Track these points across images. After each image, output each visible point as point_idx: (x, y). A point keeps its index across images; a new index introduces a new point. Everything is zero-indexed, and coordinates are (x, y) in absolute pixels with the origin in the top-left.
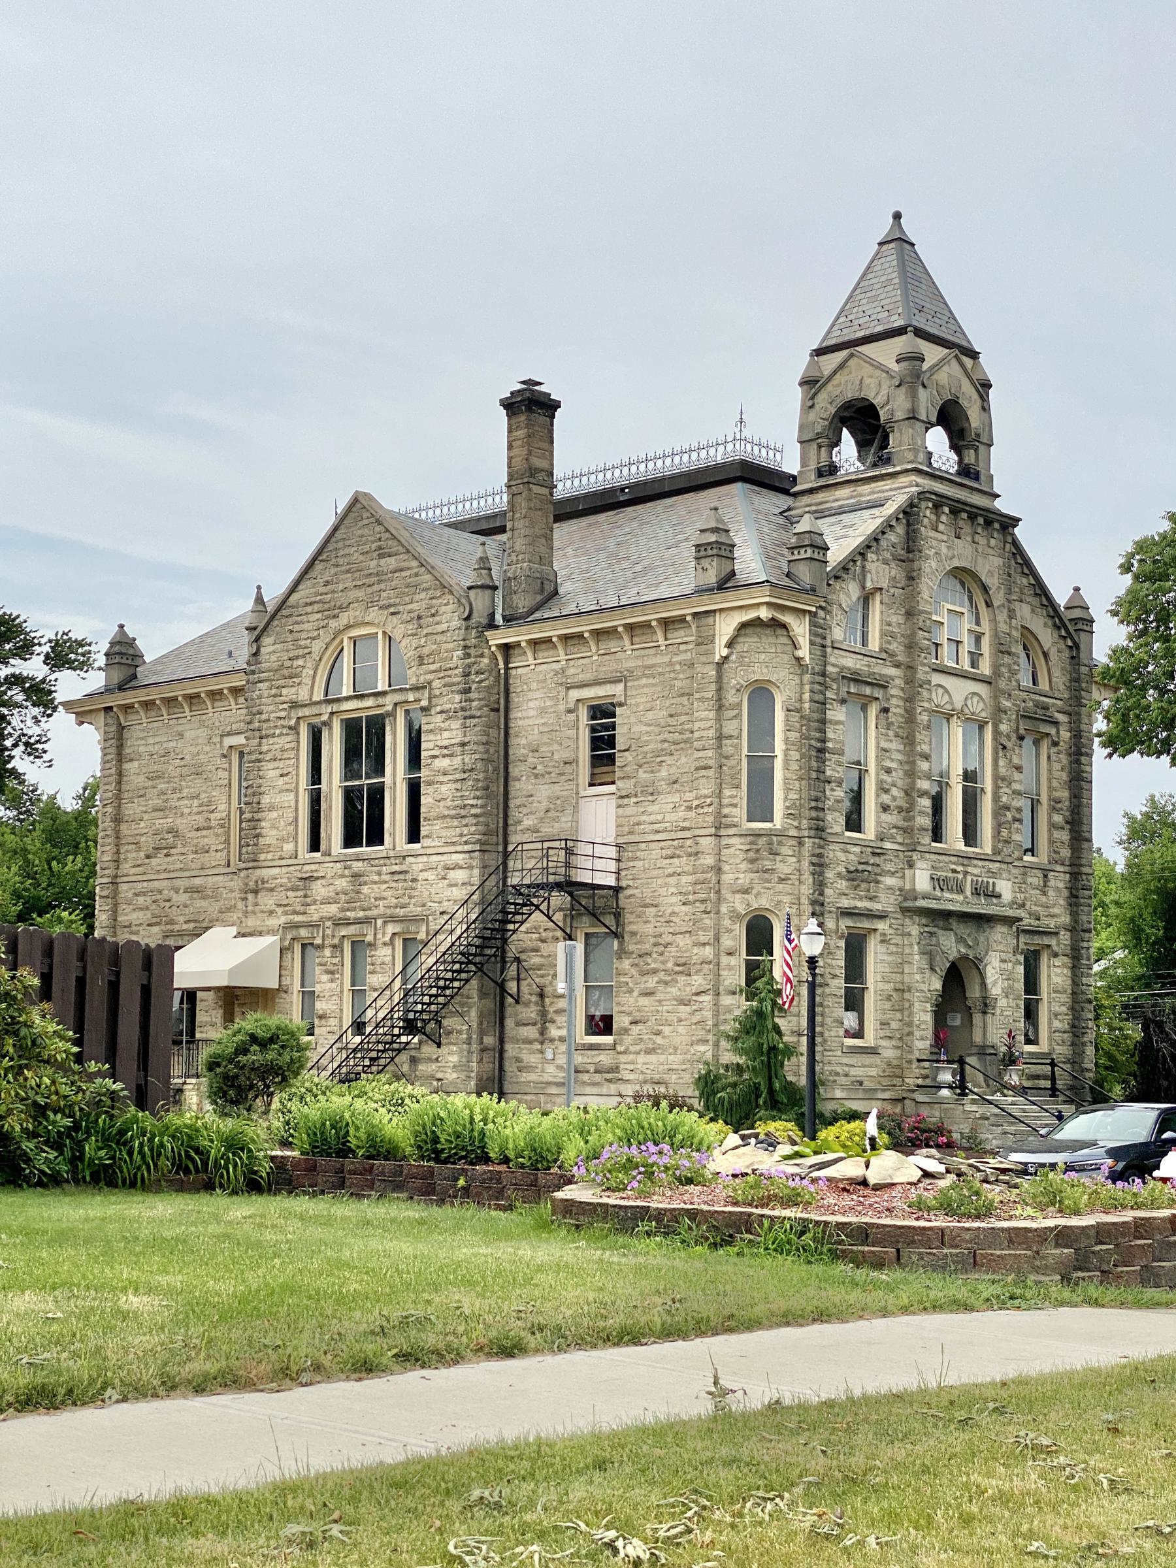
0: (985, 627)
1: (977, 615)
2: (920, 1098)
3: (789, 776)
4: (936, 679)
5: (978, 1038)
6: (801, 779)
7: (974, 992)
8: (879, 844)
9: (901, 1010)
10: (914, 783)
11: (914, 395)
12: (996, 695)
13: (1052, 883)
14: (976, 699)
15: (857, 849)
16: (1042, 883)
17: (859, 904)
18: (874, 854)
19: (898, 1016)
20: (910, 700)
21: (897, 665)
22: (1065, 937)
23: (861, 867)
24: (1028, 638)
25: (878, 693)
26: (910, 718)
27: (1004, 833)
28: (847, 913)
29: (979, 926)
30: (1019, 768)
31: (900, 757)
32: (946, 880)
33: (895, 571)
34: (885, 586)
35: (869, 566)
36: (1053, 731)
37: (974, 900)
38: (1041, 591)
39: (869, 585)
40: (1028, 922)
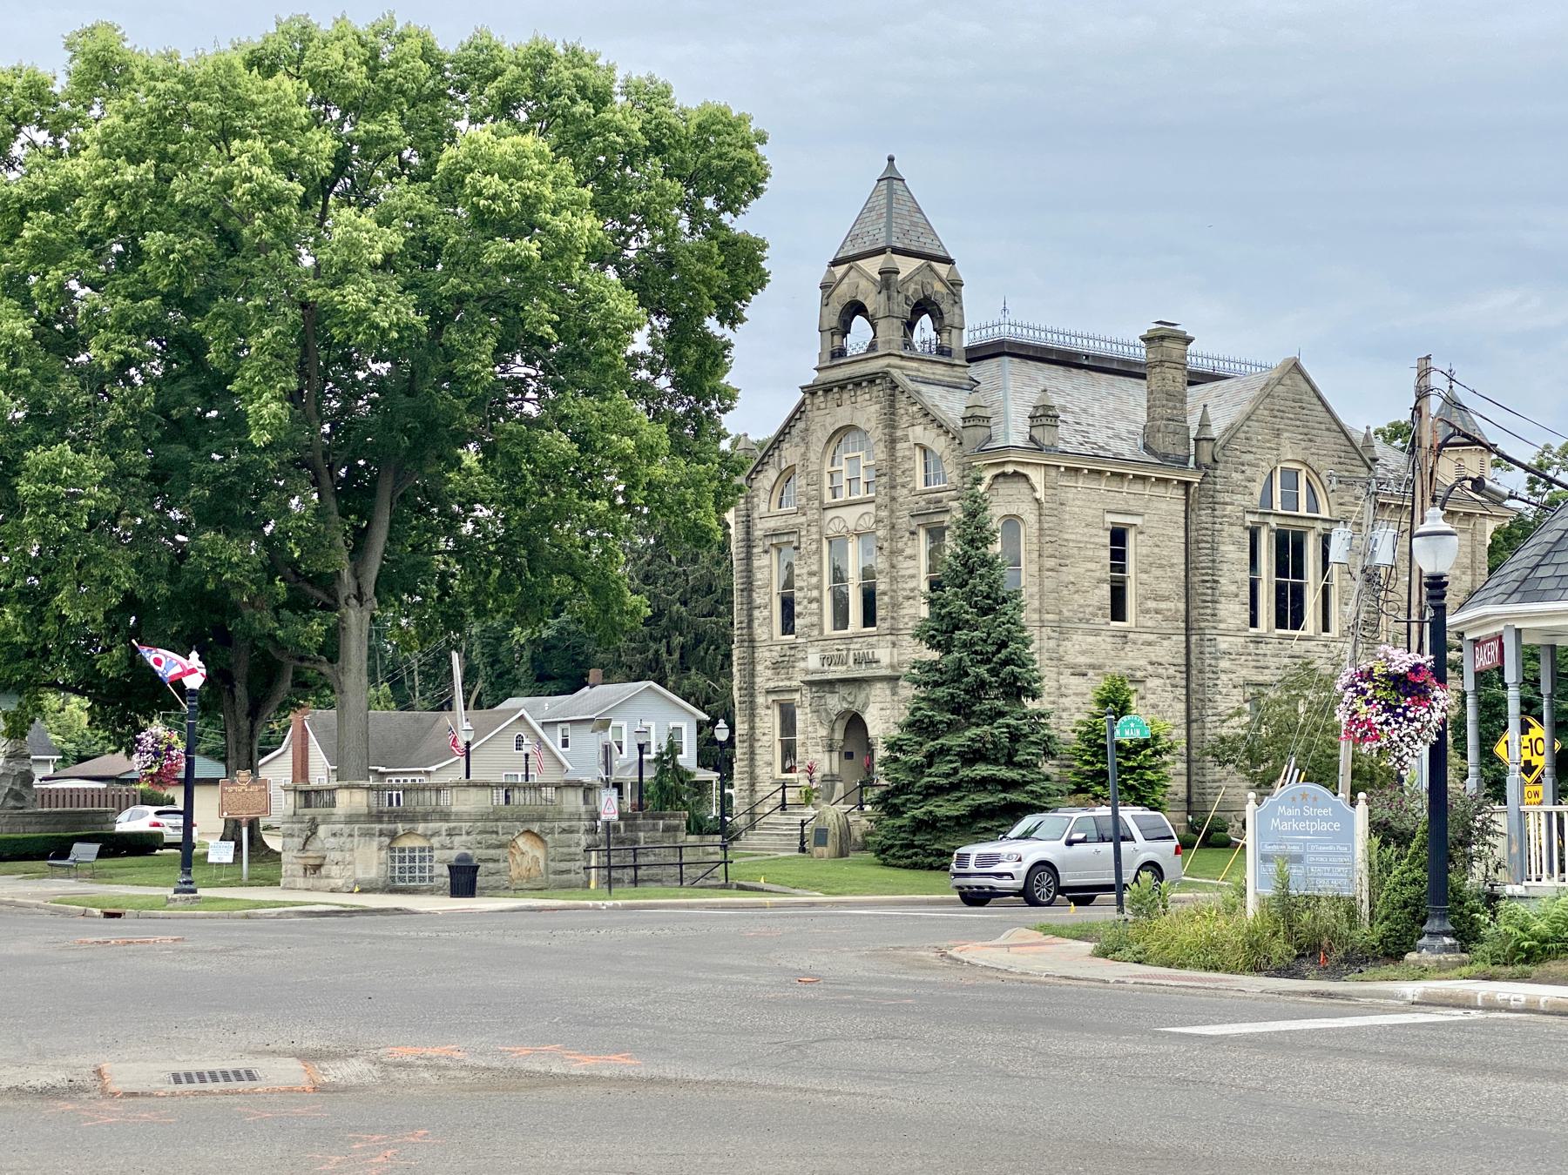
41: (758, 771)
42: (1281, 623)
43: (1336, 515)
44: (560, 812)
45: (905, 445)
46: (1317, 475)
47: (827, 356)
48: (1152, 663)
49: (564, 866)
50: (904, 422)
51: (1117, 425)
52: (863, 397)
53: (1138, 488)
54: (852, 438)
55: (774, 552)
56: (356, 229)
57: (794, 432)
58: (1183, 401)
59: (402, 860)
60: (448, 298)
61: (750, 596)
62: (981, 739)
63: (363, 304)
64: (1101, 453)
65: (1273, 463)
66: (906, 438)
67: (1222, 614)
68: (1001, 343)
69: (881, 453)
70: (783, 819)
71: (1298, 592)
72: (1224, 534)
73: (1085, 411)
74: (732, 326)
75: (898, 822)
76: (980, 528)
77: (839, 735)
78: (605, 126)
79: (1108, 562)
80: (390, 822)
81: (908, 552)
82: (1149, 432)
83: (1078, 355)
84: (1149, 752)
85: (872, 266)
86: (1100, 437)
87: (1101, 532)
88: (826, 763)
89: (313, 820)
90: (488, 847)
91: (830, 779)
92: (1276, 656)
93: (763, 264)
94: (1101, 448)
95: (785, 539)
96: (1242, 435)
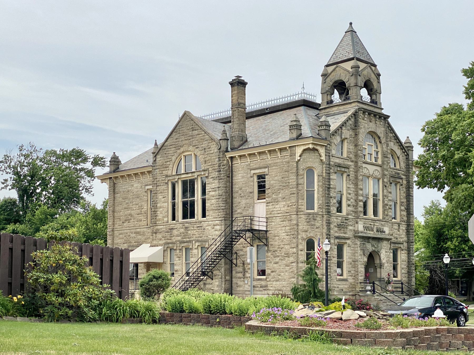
0: (379, 149)
1: (377, 146)
2: (361, 294)
3: (319, 196)
4: (364, 165)
5: (378, 276)
6: (323, 197)
7: (377, 262)
8: (347, 216)
9: (355, 267)
10: (358, 197)
11: (356, 79)
12: (383, 170)
13: (401, 228)
14: (377, 171)
15: (340, 218)
17: (341, 235)
18: (346, 219)
19: (354, 269)
20: (356, 172)
21: (352, 161)
22: (405, 244)
23: (342, 224)
24: (393, 153)
25: (346, 170)
26: (356, 178)
27: (386, 213)
28: (337, 238)
29: (379, 241)
30: (390, 193)
31: (353, 190)
32: (368, 227)
33: (351, 132)
34: (348, 137)
35: (343, 131)
36: (401, 181)
37: (377, 233)
38: (396, 138)
39: (343, 137)
40: (394, 240)
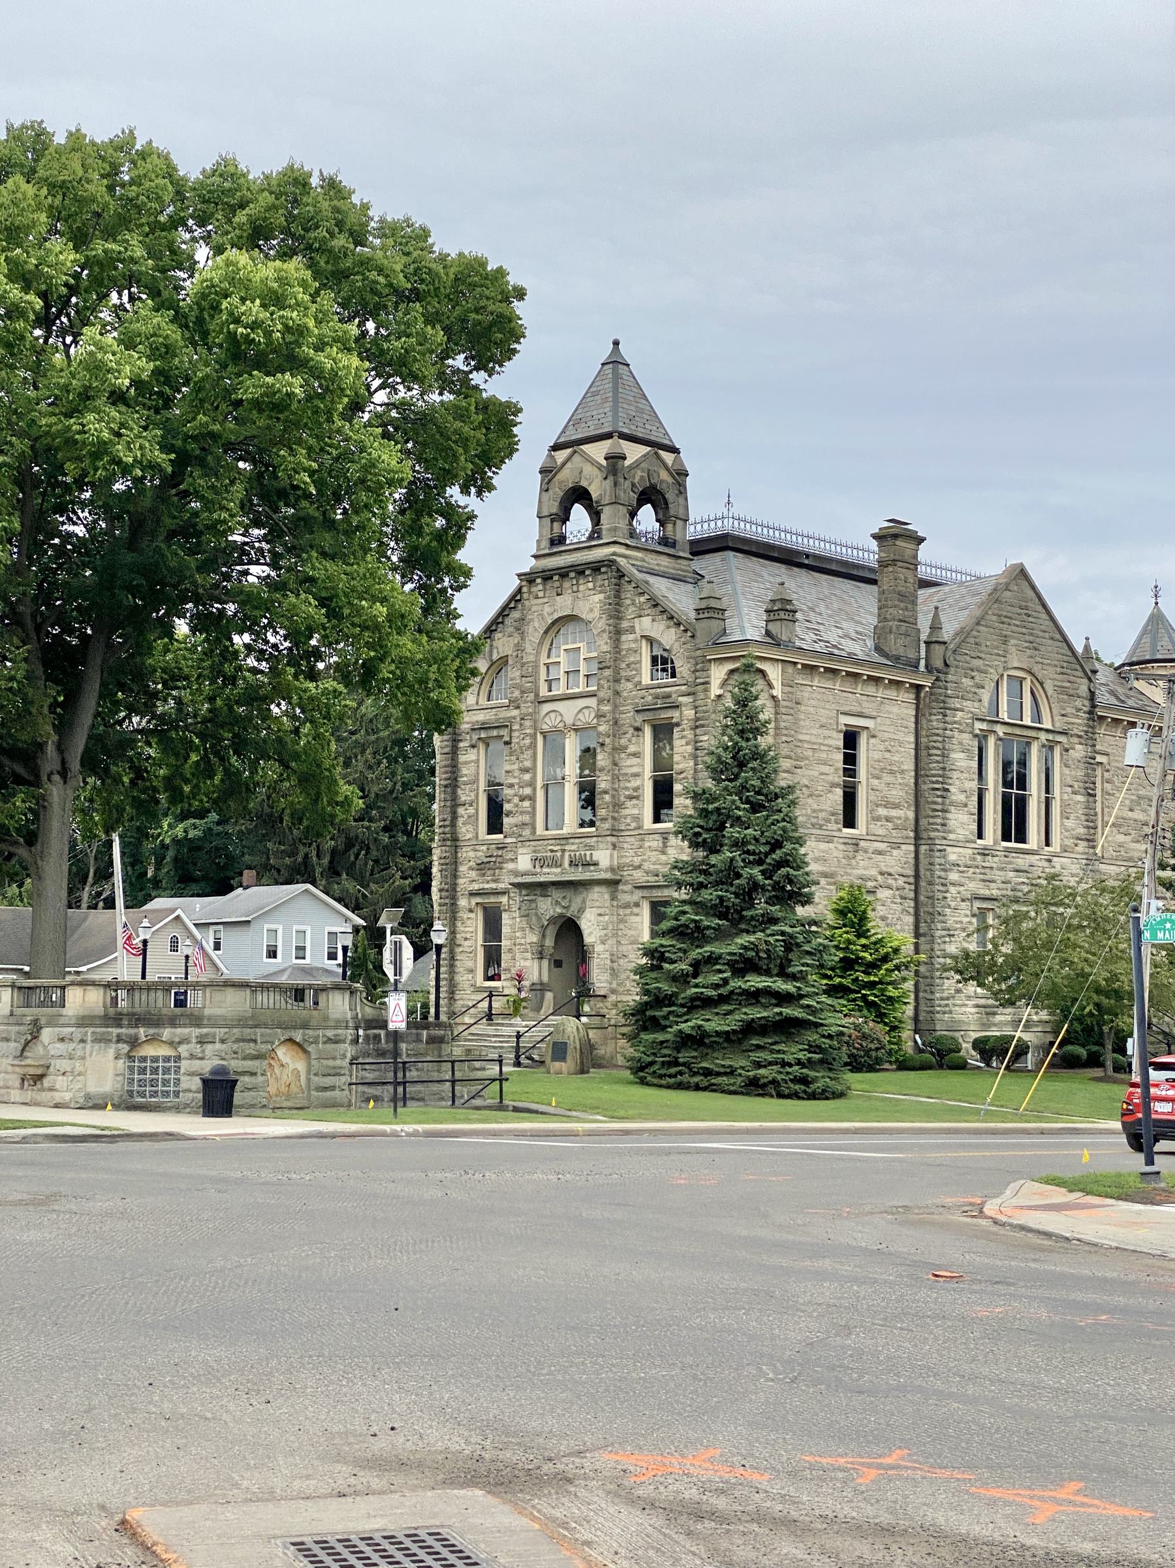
15: (484, 848)
16: (661, 845)
17: (486, 886)
18: (498, 848)
23: (486, 860)
32: (544, 859)
41: (458, 978)
42: (1006, 837)
43: (1059, 726)
44: (326, 1018)
45: (631, 637)
46: (1041, 684)
47: (545, 543)
48: (882, 874)
49: (329, 1081)
50: (630, 612)
51: (845, 625)
52: (586, 585)
53: (871, 689)
54: (570, 628)
55: (482, 746)
56: (101, 348)
57: (508, 621)
58: (914, 603)
59: (143, 1071)
60: (194, 438)
61: (454, 793)
62: (754, 947)
63: (106, 435)
64: (836, 652)
65: (1000, 671)
66: (632, 630)
67: (952, 824)
68: (725, 536)
69: (605, 644)
70: (490, 1030)
71: (1022, 802)
72: (955, 741)
73: (812, 609)
74: (479, 494)
75: (660, 1037)
76: (752, 717)
77: (549, 942)
78: (365, 263)
79: (841, 765)
80: (130, 1026)
81: (632, 749)
82: (880, 633)
83: (798, 553)
84: (889, 965)
85: (598, 451)
86: (832, 636)
87: (834, 734)
88: (535, 970)
89: (35, 1022)
90: (244, 1059)
91: (540, 989)
92: (1002, 869)
93: (515, 430)
94: (834, 646)
95: (495, 733)
96: (972, 640)
